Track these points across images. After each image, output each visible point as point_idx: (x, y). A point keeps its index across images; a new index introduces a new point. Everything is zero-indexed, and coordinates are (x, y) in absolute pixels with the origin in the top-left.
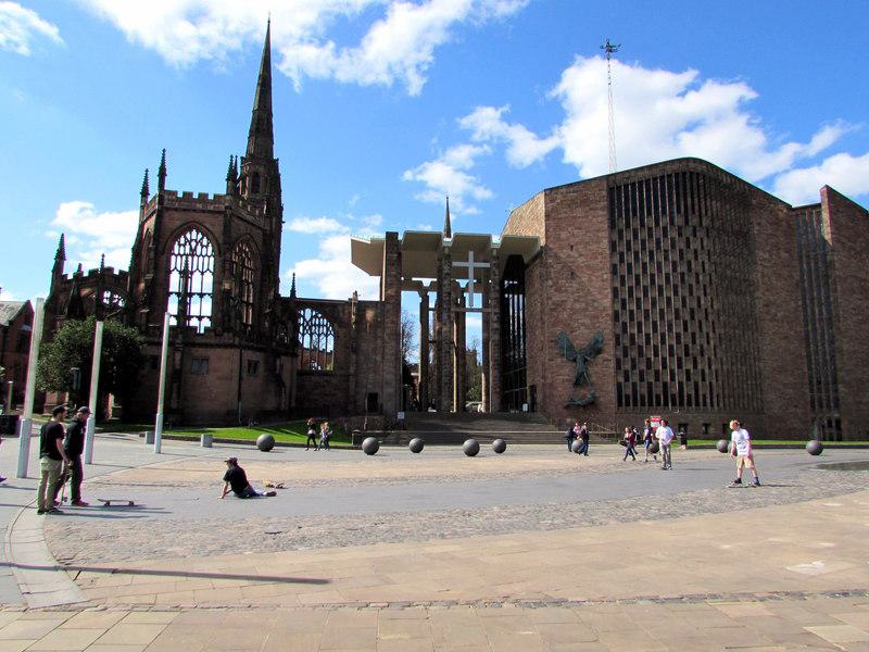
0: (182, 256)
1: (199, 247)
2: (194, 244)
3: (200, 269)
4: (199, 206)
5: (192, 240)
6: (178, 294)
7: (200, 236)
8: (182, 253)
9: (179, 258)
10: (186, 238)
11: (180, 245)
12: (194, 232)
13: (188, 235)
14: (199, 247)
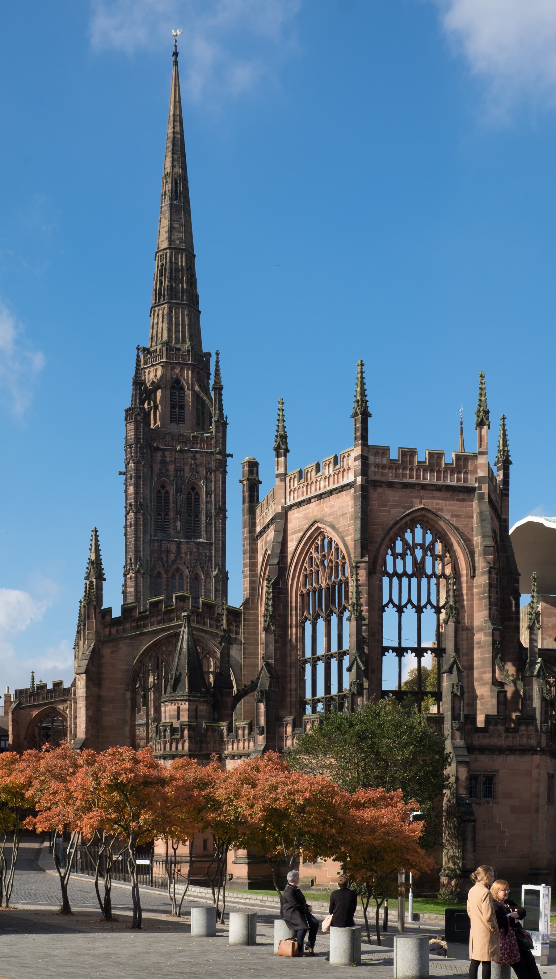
0: (400, 577)
1: (429, 560)
2: (419, 553)
3: (415, 601)
4: (430, 478)
5: (415, 545)
6: (433, 650)
7: (429, 538)
8: (400, 570)
9: (395, 580)
10: (405, 543)
11: (395, 556)
12: (419, 531)
13: (408, 536)
14: (429, 560)
